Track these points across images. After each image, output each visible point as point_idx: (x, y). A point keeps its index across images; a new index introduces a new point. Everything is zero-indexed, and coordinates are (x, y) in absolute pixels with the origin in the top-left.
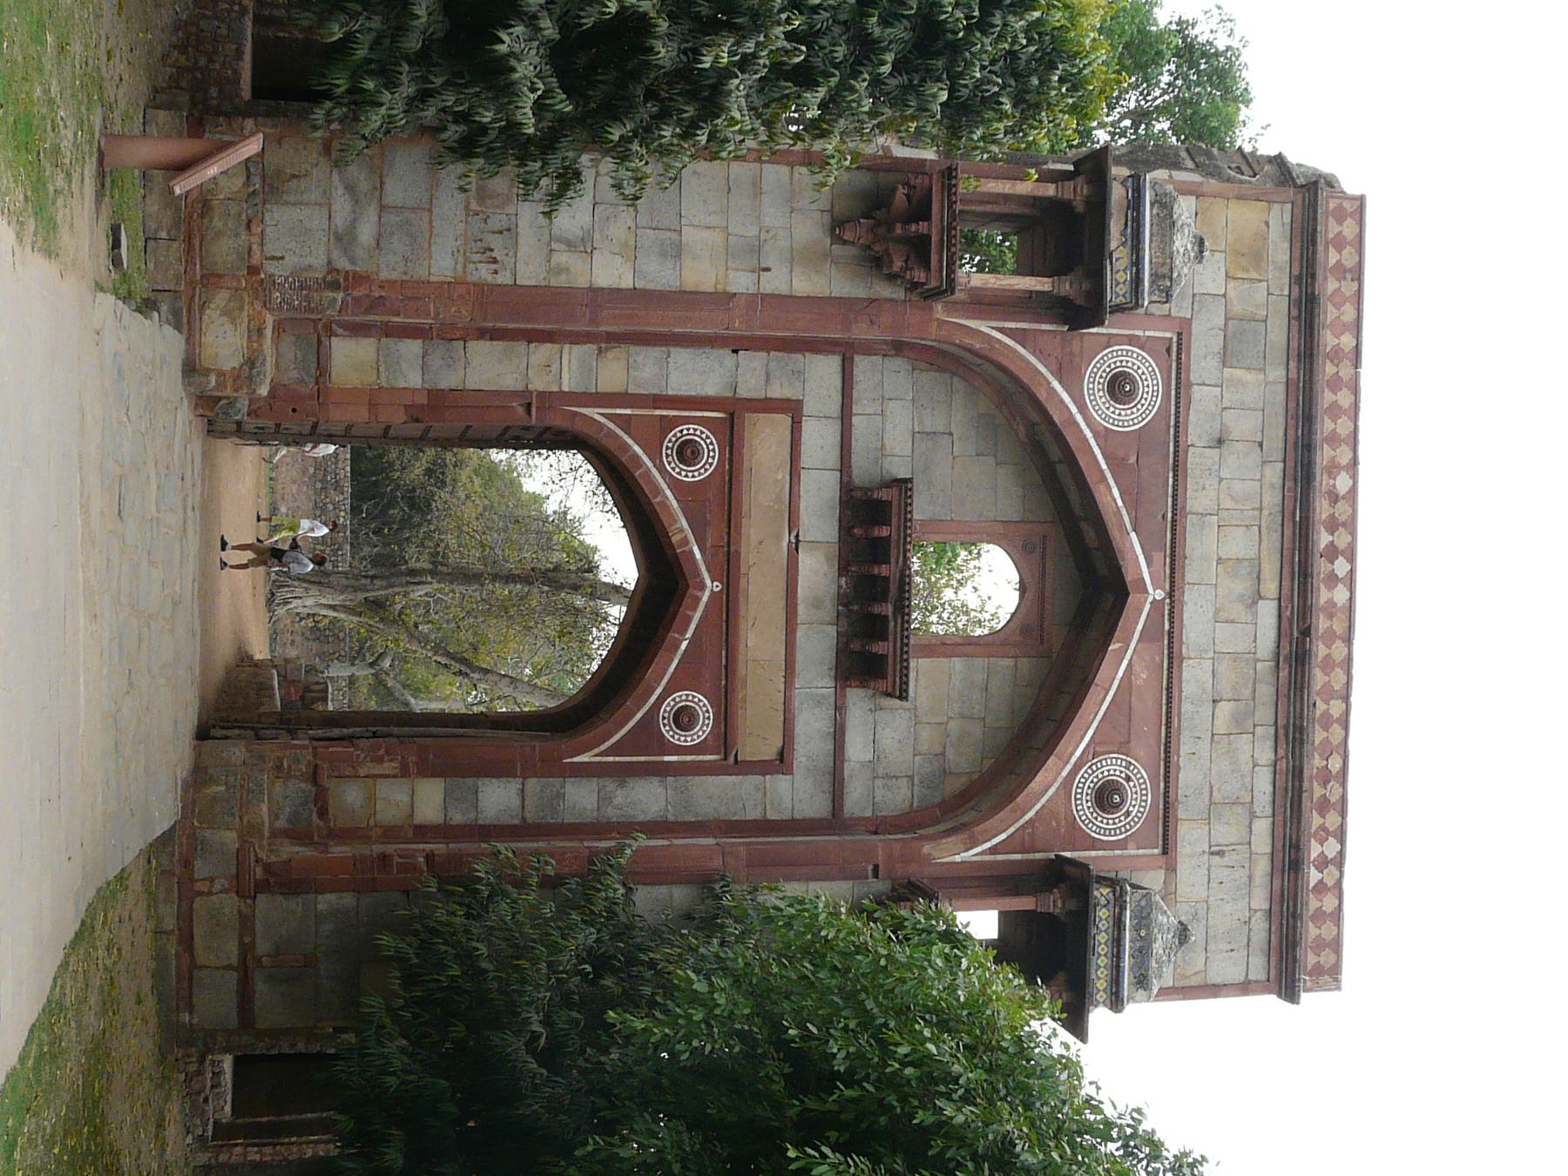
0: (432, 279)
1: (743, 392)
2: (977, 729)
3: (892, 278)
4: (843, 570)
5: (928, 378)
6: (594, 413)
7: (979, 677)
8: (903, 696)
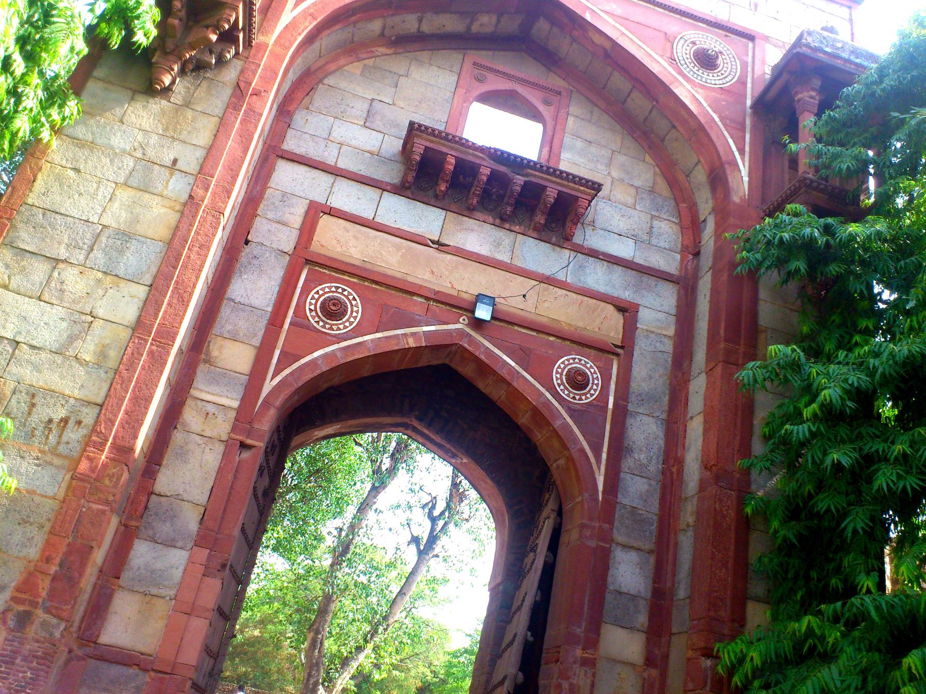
0: (61, 494)
1: (289, 247)
2: (621, 159)
3: (221, 61)
4: (468, 211)
5: (319, 99)
6: (268, 386)
7: (579, 144)
8: (596, 187)
